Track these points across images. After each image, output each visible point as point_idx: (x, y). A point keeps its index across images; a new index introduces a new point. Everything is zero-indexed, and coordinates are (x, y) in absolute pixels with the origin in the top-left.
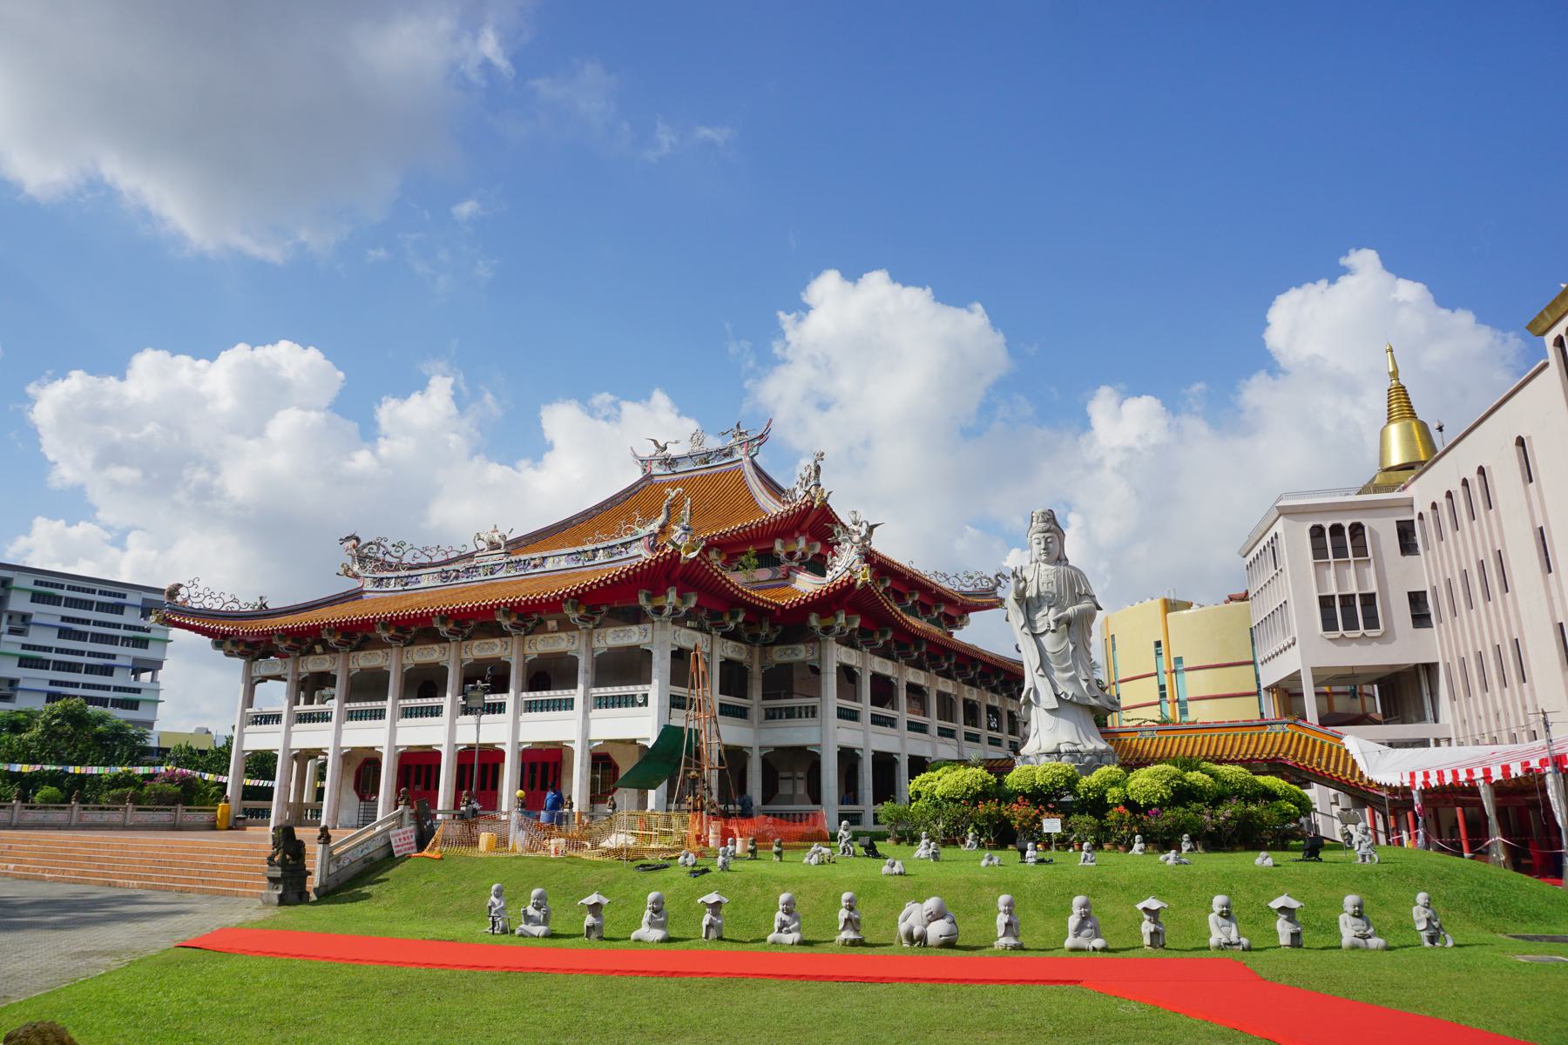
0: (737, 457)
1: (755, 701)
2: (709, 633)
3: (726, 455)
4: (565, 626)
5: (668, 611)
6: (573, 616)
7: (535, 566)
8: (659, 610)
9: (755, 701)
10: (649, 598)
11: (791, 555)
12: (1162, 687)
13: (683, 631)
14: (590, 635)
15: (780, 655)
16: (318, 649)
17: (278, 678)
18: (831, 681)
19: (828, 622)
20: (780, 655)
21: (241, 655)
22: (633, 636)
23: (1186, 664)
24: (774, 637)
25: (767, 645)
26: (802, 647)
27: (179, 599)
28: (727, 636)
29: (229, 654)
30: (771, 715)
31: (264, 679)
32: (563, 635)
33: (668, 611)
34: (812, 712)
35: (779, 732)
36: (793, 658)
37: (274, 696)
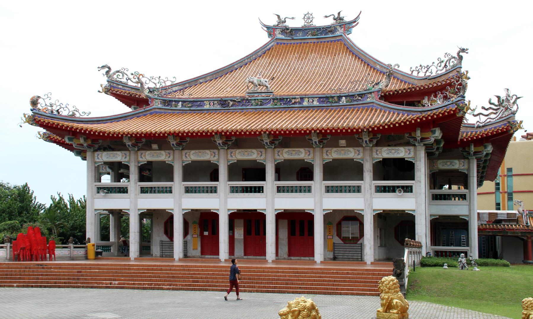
0: (338, 33)
7: (295, 103)
23: (514, 172)
26: (456, 161)
32: (351, 149)
35: (444, 207)
36: (451, 167)
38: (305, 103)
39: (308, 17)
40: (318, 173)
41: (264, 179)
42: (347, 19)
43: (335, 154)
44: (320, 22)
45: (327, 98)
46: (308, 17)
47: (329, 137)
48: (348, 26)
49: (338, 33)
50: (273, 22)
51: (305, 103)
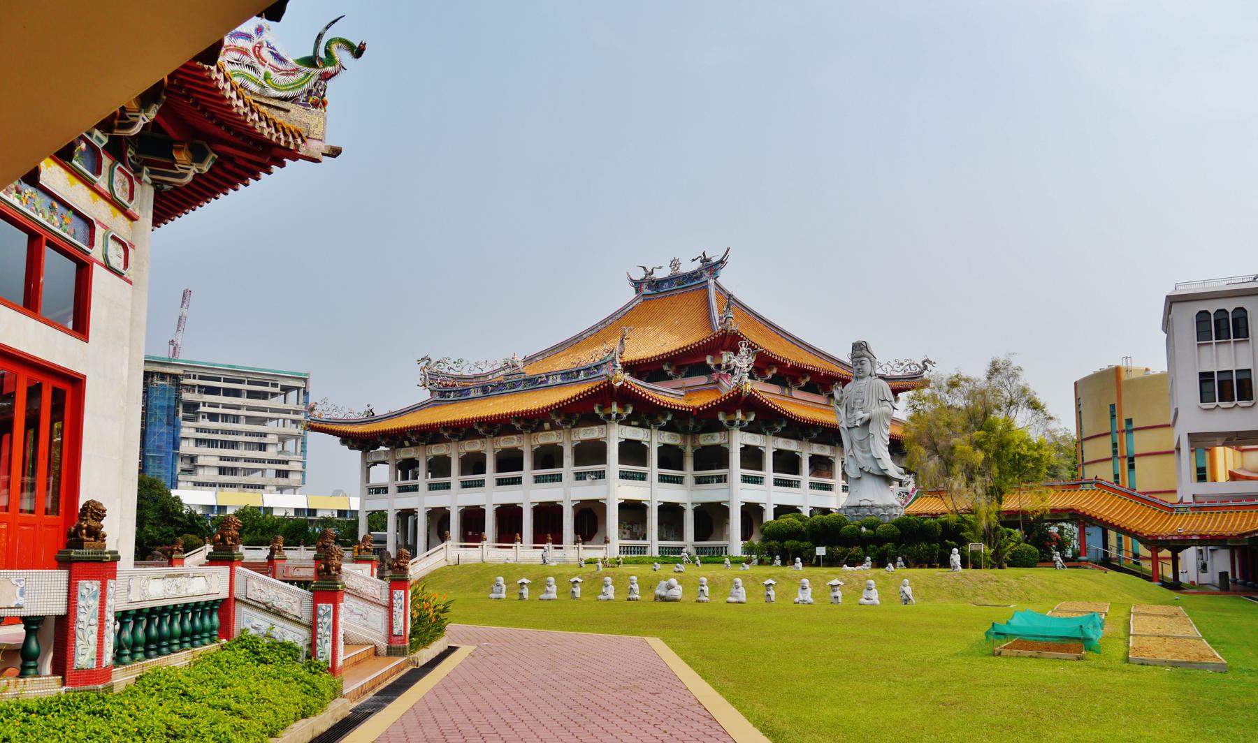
0: (704, 279)
1: (689, 472)
2: (649, 428)
3: (697, 278)
4: (554, 427)
5: (614, 416)
6: (558, 421)
8: (609, 416)
9: (689, 472)
10: (600, 409)
11: (719, 366)
12: (1115, 445)
13: (629, 428)
14: (570, 432)
15: (705, 440)
16: (407, 443)
17: (383, 462)
18: (735, 458)
19: (731, 418)
20: (705, 440)
21: (359, 448)
22: (593, 433)
23: (1135, 425)
25: (695, 433)
27: (316, 413)
28: (662, 429)
29: (351, 448)
30: (699, 481)
31: (375, 464)
33: (614, 416)
37: (382, 474)
38: (550, 382)
39: (675, 263)
40: (490, 464)
41: (484, 472)
42: (714, 260)
43: (544, 439)
44: (687, 267)
45: (567, 373)
46: (675, 263)
47: (531, 421)
48: (711, 267)
49: (704, 279)
50: (639, 275)
51: (550, 382)
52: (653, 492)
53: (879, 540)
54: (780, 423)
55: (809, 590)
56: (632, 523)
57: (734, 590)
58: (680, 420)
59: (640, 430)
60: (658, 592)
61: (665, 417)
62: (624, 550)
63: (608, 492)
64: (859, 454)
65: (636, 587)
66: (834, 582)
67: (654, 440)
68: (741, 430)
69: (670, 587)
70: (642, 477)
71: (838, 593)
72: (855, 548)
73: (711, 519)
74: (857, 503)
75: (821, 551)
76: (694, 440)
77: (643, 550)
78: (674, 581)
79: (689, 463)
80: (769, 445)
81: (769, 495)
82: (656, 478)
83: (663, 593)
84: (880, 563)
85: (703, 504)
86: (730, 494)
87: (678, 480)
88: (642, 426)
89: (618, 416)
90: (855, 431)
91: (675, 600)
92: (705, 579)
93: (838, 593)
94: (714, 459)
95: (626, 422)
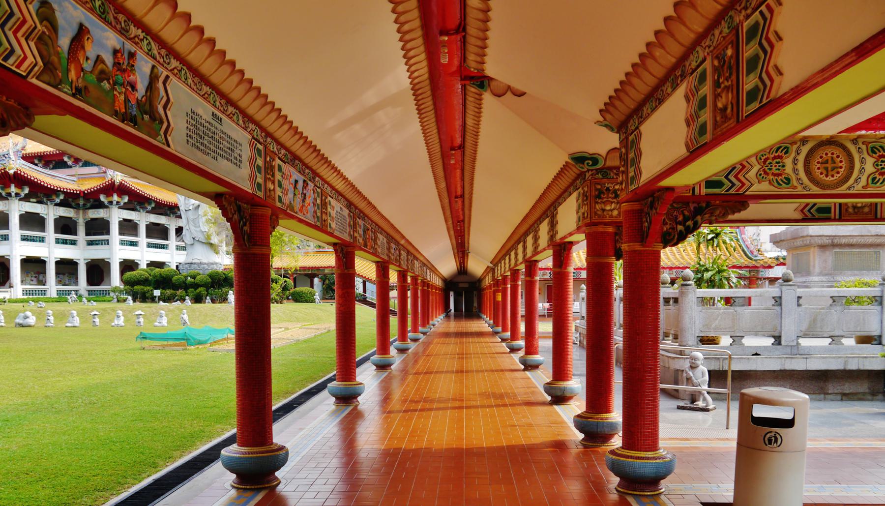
1: (81, 236)
9: (81, 236)
13: (27, 203)
19: (110, 199)
24: (89, 205)
30: (90, 243)
34: (107, 242)
52: (51, 250)
53: (196, 286)
54: (150, 204)
55: (122, 318)
56: (39, 273)
57: (71, 319)
58: (70, 199)
59: (39, 205)
60: (17, 321)
61: (58, 196)
62: (26, 292)
63: (11, 251)
64: (192, 228)
65: (51, 318)
66: (138, 312)
67: (51, 213)
68: (119, 208)
69: (26, 317)
70: (42, 240)
71: (141, 320)
72: (180, 291)
73: (98, 271)
74: (190, 261)
75: (157, 293)
76: (84, 214)
77: (44, 292)
78: (29, 313)
79: (81, 230)
80: (143, 219)
81: (143, 254)
82: (53, 241)
83: (21, 322)
84: (198, 299)
85: (92, 260)
86: (111, 253)
87: (73, 243)
88: (40, 202)
89: (17, 195)
90: (190, 212)
91: (30, 326)
92: (50, 312)
93: (141, 320)
94: (98, 228)
95: (26, 198)
